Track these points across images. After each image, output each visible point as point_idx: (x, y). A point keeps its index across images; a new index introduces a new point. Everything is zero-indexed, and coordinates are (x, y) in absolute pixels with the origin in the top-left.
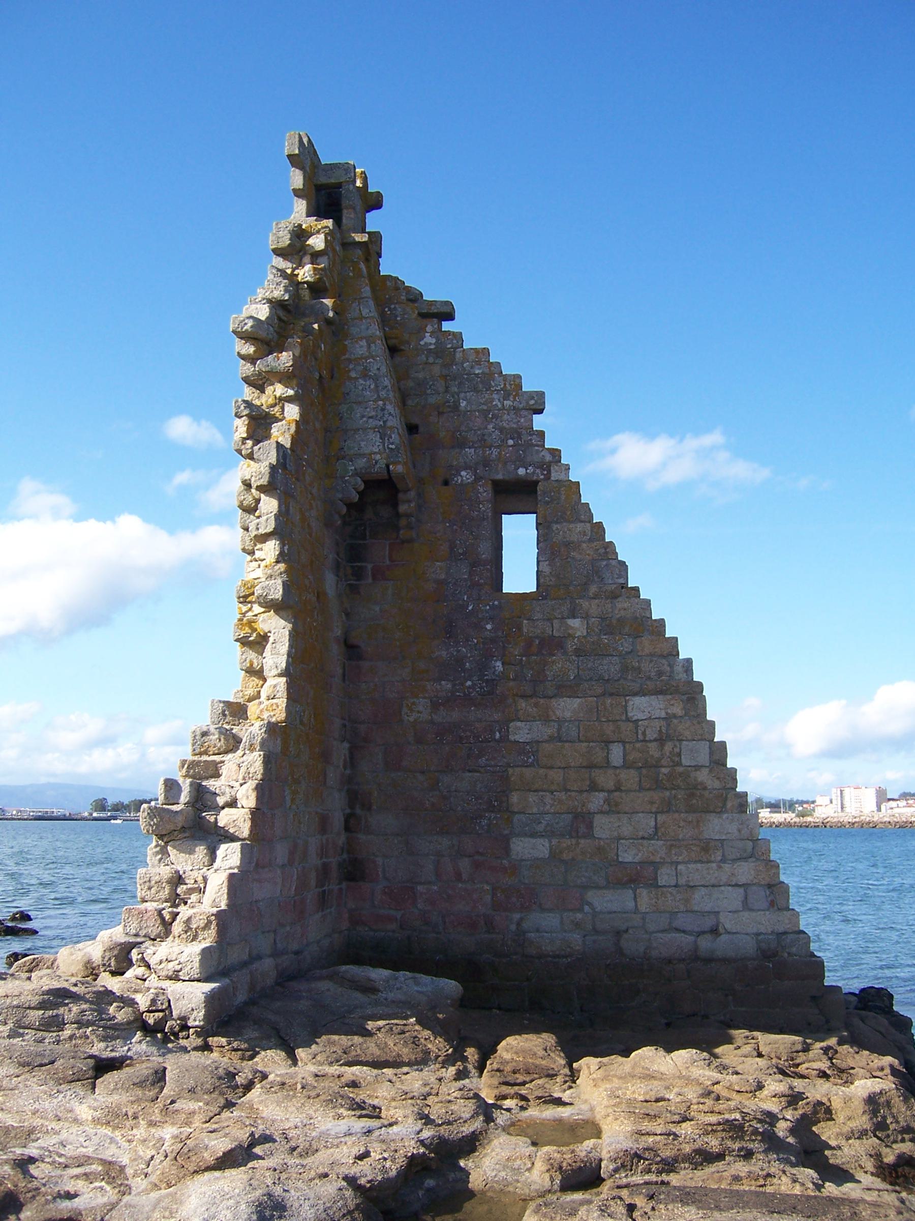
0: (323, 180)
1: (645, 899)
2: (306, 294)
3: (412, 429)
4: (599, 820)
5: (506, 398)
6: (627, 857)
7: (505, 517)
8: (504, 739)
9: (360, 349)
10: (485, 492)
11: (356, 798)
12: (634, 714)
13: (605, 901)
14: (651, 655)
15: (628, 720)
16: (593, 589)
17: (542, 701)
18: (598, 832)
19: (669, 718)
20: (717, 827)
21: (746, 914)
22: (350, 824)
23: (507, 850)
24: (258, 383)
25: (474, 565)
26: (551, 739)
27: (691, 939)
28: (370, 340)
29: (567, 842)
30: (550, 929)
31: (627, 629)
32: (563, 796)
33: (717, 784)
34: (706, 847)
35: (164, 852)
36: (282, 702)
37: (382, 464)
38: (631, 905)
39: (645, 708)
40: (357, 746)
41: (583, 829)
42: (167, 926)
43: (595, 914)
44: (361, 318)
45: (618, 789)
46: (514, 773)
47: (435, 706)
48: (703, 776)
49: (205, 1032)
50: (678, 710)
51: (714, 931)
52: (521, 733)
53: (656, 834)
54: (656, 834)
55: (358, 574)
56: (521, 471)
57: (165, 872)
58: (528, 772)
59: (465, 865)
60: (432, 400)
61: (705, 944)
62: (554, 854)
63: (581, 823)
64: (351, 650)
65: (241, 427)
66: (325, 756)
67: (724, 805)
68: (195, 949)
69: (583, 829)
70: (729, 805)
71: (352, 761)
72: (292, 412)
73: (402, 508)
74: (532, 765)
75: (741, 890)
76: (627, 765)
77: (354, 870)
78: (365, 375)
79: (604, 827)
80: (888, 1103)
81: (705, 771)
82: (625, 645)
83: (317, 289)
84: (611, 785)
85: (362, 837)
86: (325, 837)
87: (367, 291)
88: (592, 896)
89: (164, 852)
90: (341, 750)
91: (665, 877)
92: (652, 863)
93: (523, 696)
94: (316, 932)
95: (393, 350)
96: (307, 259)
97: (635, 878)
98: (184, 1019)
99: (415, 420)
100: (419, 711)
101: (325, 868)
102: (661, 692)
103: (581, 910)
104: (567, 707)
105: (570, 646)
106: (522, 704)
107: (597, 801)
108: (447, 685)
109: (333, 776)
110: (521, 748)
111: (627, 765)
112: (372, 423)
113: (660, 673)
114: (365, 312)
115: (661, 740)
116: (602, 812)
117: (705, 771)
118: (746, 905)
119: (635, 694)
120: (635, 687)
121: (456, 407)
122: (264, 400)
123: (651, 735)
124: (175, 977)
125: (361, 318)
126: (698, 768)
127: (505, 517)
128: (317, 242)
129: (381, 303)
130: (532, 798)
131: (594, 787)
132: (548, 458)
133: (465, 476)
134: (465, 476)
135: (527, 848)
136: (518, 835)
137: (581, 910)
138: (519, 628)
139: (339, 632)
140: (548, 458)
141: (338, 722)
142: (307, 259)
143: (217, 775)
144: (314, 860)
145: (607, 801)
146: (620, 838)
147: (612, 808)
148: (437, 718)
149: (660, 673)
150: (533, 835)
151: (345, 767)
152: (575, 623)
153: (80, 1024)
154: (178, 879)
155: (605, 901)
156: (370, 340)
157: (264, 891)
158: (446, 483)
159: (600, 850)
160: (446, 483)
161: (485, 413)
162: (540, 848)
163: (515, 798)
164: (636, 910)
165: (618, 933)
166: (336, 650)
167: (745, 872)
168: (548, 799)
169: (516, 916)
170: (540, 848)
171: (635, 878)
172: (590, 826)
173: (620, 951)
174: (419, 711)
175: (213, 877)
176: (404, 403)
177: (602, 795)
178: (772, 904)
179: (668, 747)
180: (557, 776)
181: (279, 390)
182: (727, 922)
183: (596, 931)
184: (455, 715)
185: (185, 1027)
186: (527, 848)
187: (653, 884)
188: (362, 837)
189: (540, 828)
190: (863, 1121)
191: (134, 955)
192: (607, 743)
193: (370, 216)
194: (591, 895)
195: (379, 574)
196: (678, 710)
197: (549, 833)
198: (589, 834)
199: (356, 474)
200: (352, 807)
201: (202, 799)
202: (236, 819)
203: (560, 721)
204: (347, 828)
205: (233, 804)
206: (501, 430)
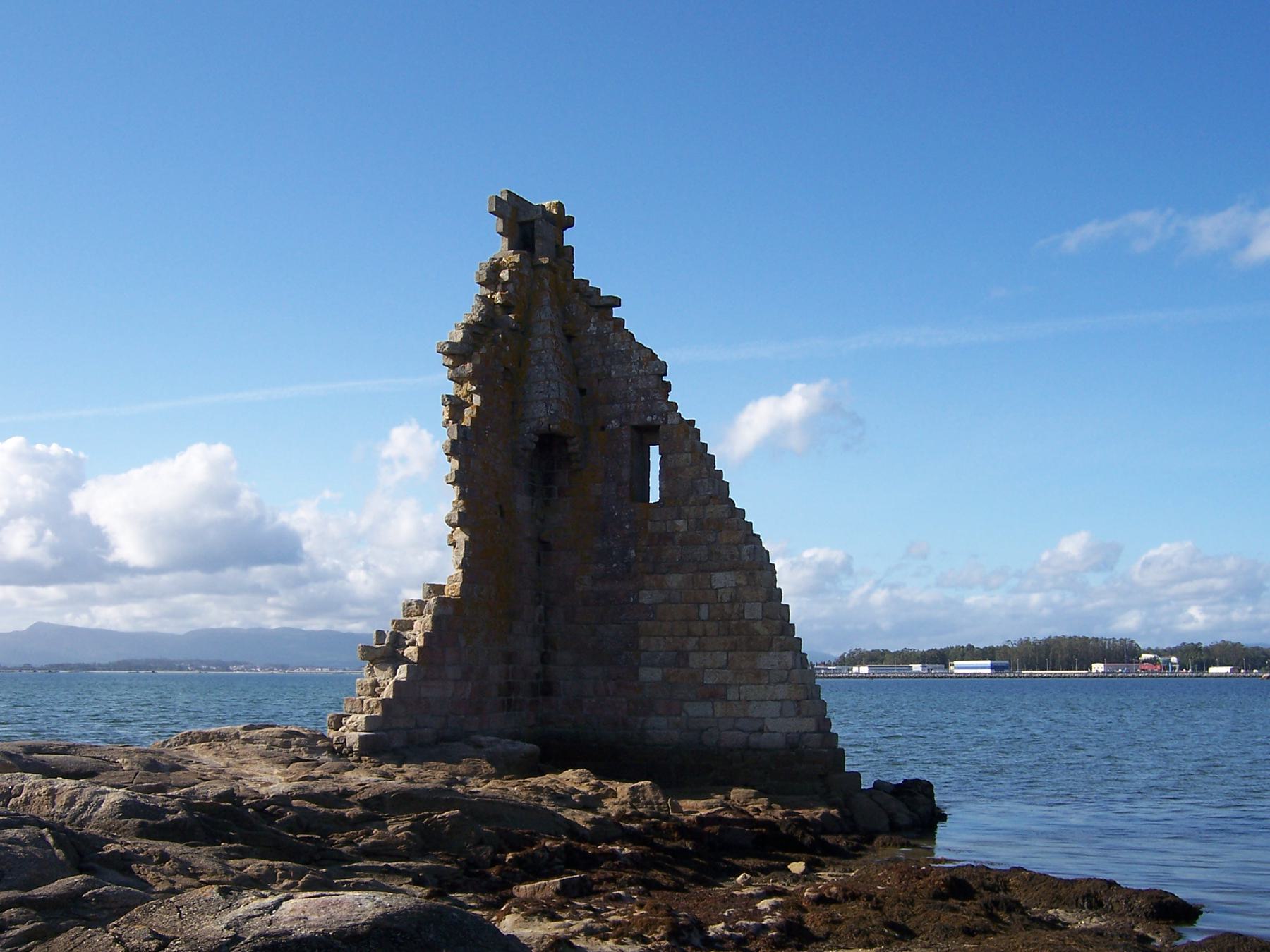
0: (523, 219)
1: (719, 706)
2: (499, 311)
3: (583, 392)
4: (692, 656)
5: (640, 367)
6: (709, 681)
8: (636, 601)
9: (537, 343)
12: (716, 585)
13: (697, 710)
14: (728, 544)
15: (712, 588)
16: (692, 499)
17: (659, 576)
18: (691, 664)
19: (737, 587)
20: (768, 661)
21: (781, 720)
22: (544, 659)
23: (637, 675)
24: (459, 381)
27: (742, 735)
28: (544, 337)
30: (661, 728)
31: (712, 527)
32: (670, 639)
33: (766, 632)
34: (759, 675)
35: (371, 670)
36: (458, 584)
37: (545, 424)
39: (721, 580)
44: (540, 321)
45: (705, 635)
48: (758, 626)
49: (360, 754)
50: (742, 581)
51: (761, 731)
52: (646, 598)
53: (726, 666)
54: (726, 666)
56: (649, 418)
57: (369, 680)
61: (754, 739)
63: (682, 657)
64: (545, 545)
65: (444, 413)
67: (771, 646)
70: (774, 646)
72: (477, 400)
74: (651, 620)
75: (779, 704)
76: (710, 619)
77: (545, 689)
78: (539, 363)
79: (695, 660)
80: (644, 791)
81: (759, 623)
82: (711, 538)
83: (507, 307)
86: (511, 667)
87: (546, 299)
89: (371, 670)
91: (732, 693)
92: (725, 685)
93: (648, 573)
95: (570, 338)
96: (499, 287)
97: (714, 694)
98: (351, 747)
99: (584, 386)
102: (734, 569)
103: (680, 715)
104: (674, 580)
105: (677, 538)
106: (647, 578)
107: (691, 643)
108: (602, 567)
111: (710, 619)
113: (733, 556)
114: (543, 317)
115: (732, 602)
116: (694, 651)
117: (759, 623)
118: (782, 714)
119: (717, 571)
121: (610, 374)
122: (461, 393)
123: (726, 599)
125: (540, 321)
126: (755, 620)
128: (504, 275)
131: (690, 634)
132: (666, 408)
134: (615, 423)
137: (680, 715)
140: (666, 408)
142: (499, 287)
145: (698, 643)
146: (705, 668)
147: (701, 648)
149: (733, 556)
150: (653, 666)
151: (540, 620)
152: (680, 523)
153: (298, 745)
154: (376, 684)
155: (697, 710)
156: (544, 337)
158: (603, 428)
161: (627, 379)
163: (642, 641)
165: (702, 731)
167: (782, 691)
169: (641, 719)
171: (714, 694)
172: (687, 660)
175: (388, 681)
178: (799, 713)
179: (737, 606)
181: (469, 386)
185: (351, 751)
186: (649, 674)
187: (724, 698)
190: (627, 798)
192: (699, 604)
196: (742, 581)
199: (530, 432)
201: (398, 640)
202: (411, 652)
205: (413, 644)
206: (636, 389)
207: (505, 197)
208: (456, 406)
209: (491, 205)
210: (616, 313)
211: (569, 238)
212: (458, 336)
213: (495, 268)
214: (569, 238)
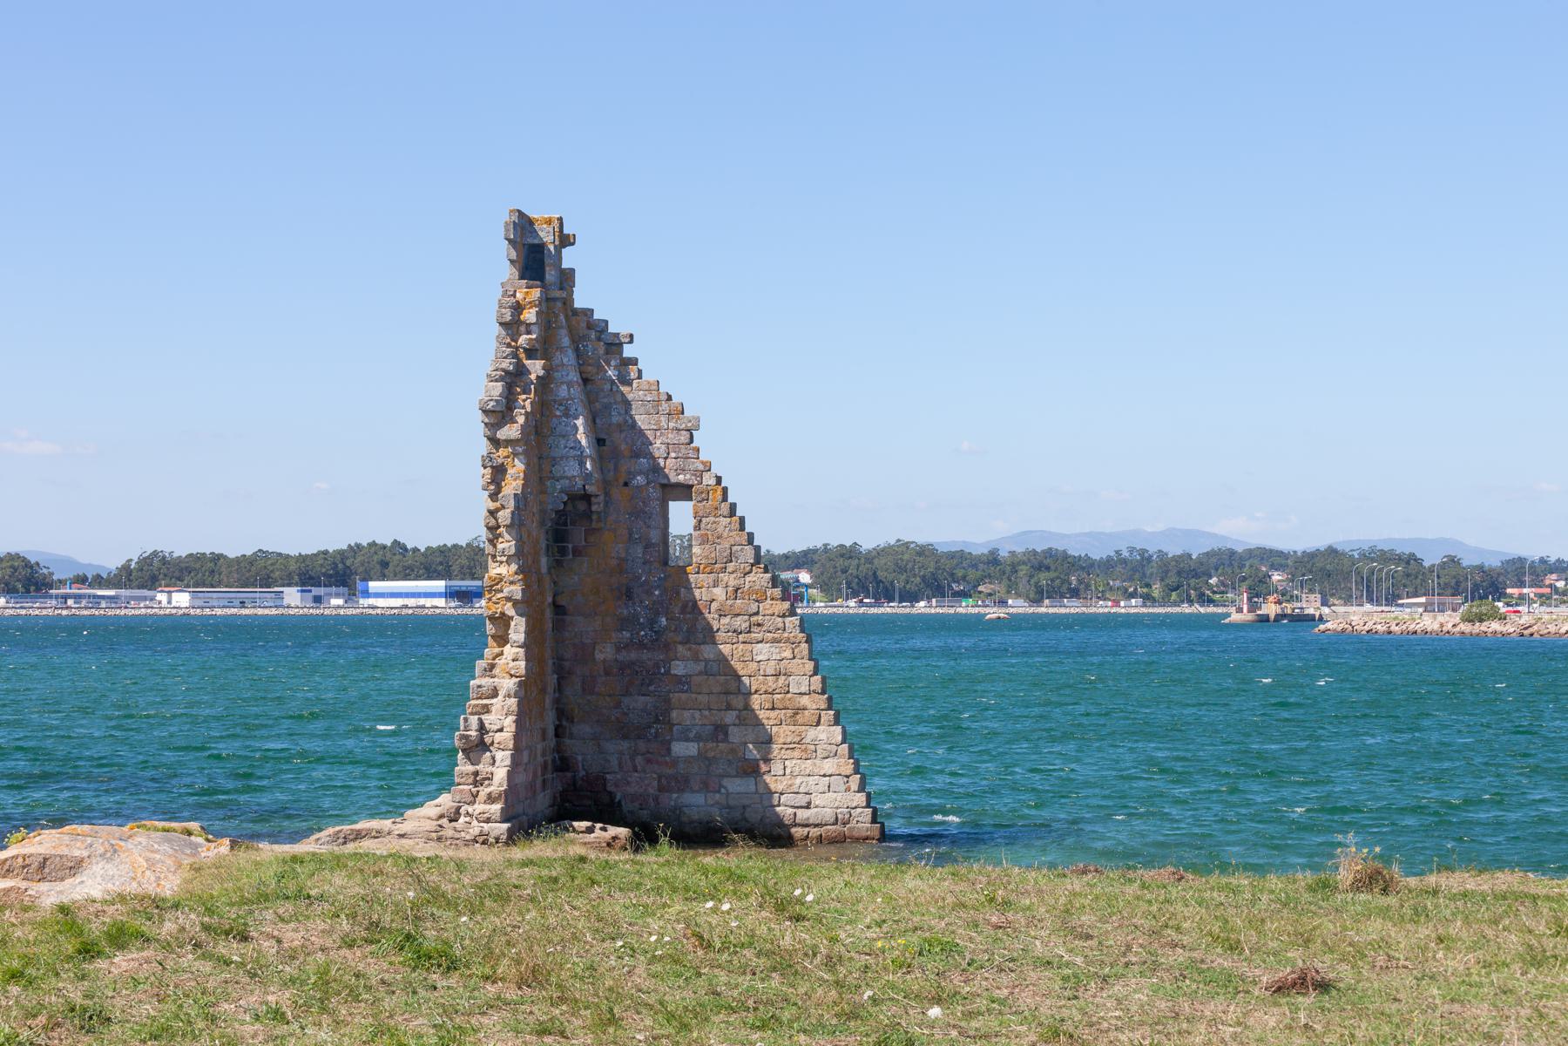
7: (671, 504)
8: (668, 672)
9: (563, 392)
10: (654, 493)
11: (562, 713)
16: (731, 566)
23: (669, 750)
25: (646, 547)
26: (700, 673)
27: (791, 811)
28: (570, 384)
29: (711, 745)
36: (522, 664)
38: (753, 788)
40: (562, 675)
41: (721, 737)
42: (475, 796)
43: (728, 794)
46: (675, 697)
47: (618, 650)
52: (679, 669)
55: (563, 551)
56: (681, 477)
58: (684, 696)
59: (639, 759)
60: (615, 420)
61: (802, 815)
62: (701, 755)
63: (720, 731)
64: (558, 609)
66: (543, 691)
68: (496, 808)
69: (721, 737)
71: (559, 688)
73: (594, 508)
82: (754, 607)
84: (741, 706)
85: (568, 741)
87: (566, 341)
88: (725, 782)
90: (552, 679)
94: (543, 802)
95: (585, 381)
100: (604, 653)
101: (545, 762)
106: (680, 648)
107: (730, 717)
109: (548, 701)
110: (679, 680)
112: (572, 453)
115: (777, 675)
120: (759, 636)
123: (770, 671)
124: (488, 821)
127: (671, 504)
128: (530, 315)
129: (576, 340)
130: (687, 714)
131: (729, 708)
132: (701, 467)
133: (640, 479)
134: (640, 479)
135: (681, 749)
136: (678, 740)
138: (678, 593)
139: (550, 600)
141: (550, 662)
143: (488, 712)
144: (540, 759)
145: (738, 717)
148: (620, 658)
150: (687, 740)
155: (735, 785)
156: (570, 384)
157: (521, 778)
158: (626, 484)
159: (733, 751)
160: (626, 484)
162: (691, 749)
163: (674, 714)
164: (757, 792)
165: (744, 807)
166: (549, 613)
167: (829, 766)
168: (697, 714)
170: (691, 749)
172: (726, 734)
173: (746, 820)
174: (604, 653)
176: (594, 421)
177: (735, 713)
180: (703, 699)
182: (817, 800)
183: (729, 807)
184: (633, 656)
186: (683, 749)
188: (568, 741)
189: (692, 735)
191: (462, 811)
193: (566, 252)
194: (725, 782)
195: (577, 552)
196: (788, 654)
197: (698, 738)
198: (726, 740)
199: (562, 491)
200: (559, 719)
203: (707, 661)
204: (557, 735)
207: (515, 218)
208: (498, 473)
209: (507, 230)
210: (628, 352)
211: (569, 258)
212: (498, 388)
213: (518, 308)
214: (569, 258)
